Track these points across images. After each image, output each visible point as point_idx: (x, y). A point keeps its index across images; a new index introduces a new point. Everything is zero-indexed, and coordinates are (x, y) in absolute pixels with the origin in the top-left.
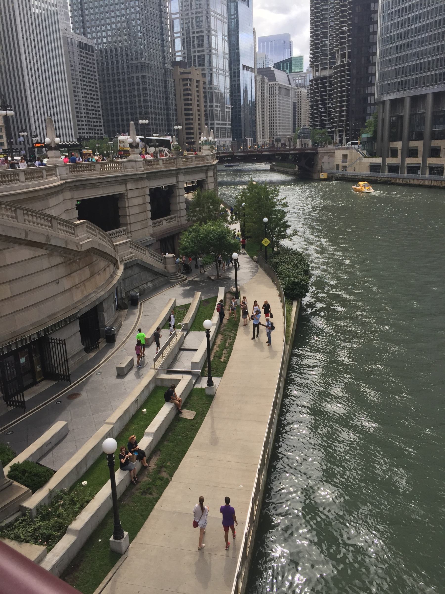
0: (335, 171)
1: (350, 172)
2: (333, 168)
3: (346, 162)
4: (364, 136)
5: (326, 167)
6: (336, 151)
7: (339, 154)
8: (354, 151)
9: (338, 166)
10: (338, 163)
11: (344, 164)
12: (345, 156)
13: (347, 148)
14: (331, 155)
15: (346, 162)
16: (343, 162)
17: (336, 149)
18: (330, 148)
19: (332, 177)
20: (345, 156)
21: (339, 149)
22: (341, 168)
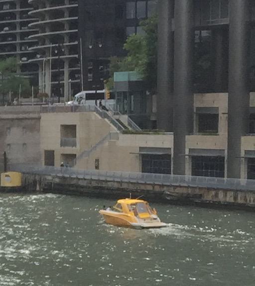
0: (42, 166)
1: (82, 170)
2: (36, 160)
3: (74, 145)
4: (120, 77)
5: (15, 155)
6: (45, 117)
7: (51, 125)
8: (95, 116)
9: (50, 156)
10: (50, 148)
11: (68, 150)
12: (69, 130)
13: (74, 109)
14: (32, 125)
15: (74, 145)
16: (63, 144)
17: (45, 110)
18: (28, 106)
19: (35, 182)
20: (69, 130)
21: (53, 110)
22: (58, 161)
